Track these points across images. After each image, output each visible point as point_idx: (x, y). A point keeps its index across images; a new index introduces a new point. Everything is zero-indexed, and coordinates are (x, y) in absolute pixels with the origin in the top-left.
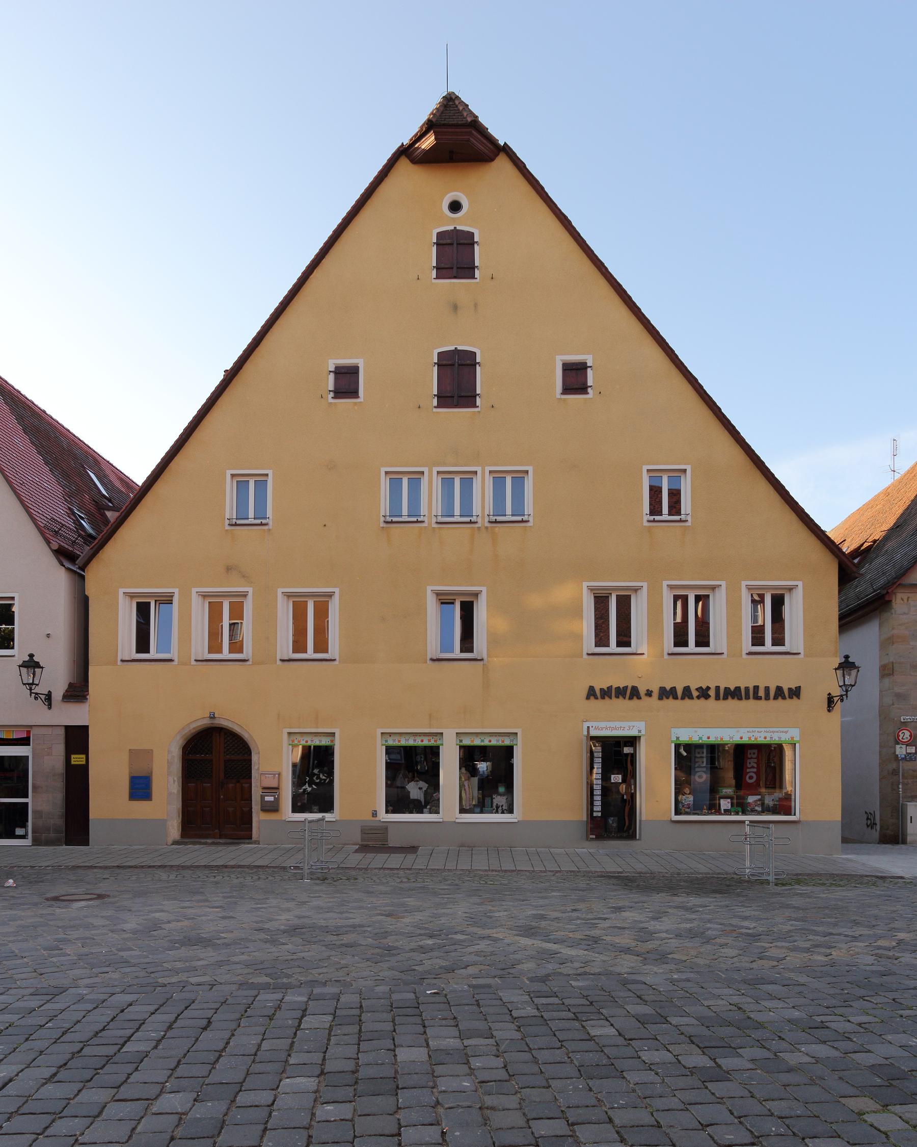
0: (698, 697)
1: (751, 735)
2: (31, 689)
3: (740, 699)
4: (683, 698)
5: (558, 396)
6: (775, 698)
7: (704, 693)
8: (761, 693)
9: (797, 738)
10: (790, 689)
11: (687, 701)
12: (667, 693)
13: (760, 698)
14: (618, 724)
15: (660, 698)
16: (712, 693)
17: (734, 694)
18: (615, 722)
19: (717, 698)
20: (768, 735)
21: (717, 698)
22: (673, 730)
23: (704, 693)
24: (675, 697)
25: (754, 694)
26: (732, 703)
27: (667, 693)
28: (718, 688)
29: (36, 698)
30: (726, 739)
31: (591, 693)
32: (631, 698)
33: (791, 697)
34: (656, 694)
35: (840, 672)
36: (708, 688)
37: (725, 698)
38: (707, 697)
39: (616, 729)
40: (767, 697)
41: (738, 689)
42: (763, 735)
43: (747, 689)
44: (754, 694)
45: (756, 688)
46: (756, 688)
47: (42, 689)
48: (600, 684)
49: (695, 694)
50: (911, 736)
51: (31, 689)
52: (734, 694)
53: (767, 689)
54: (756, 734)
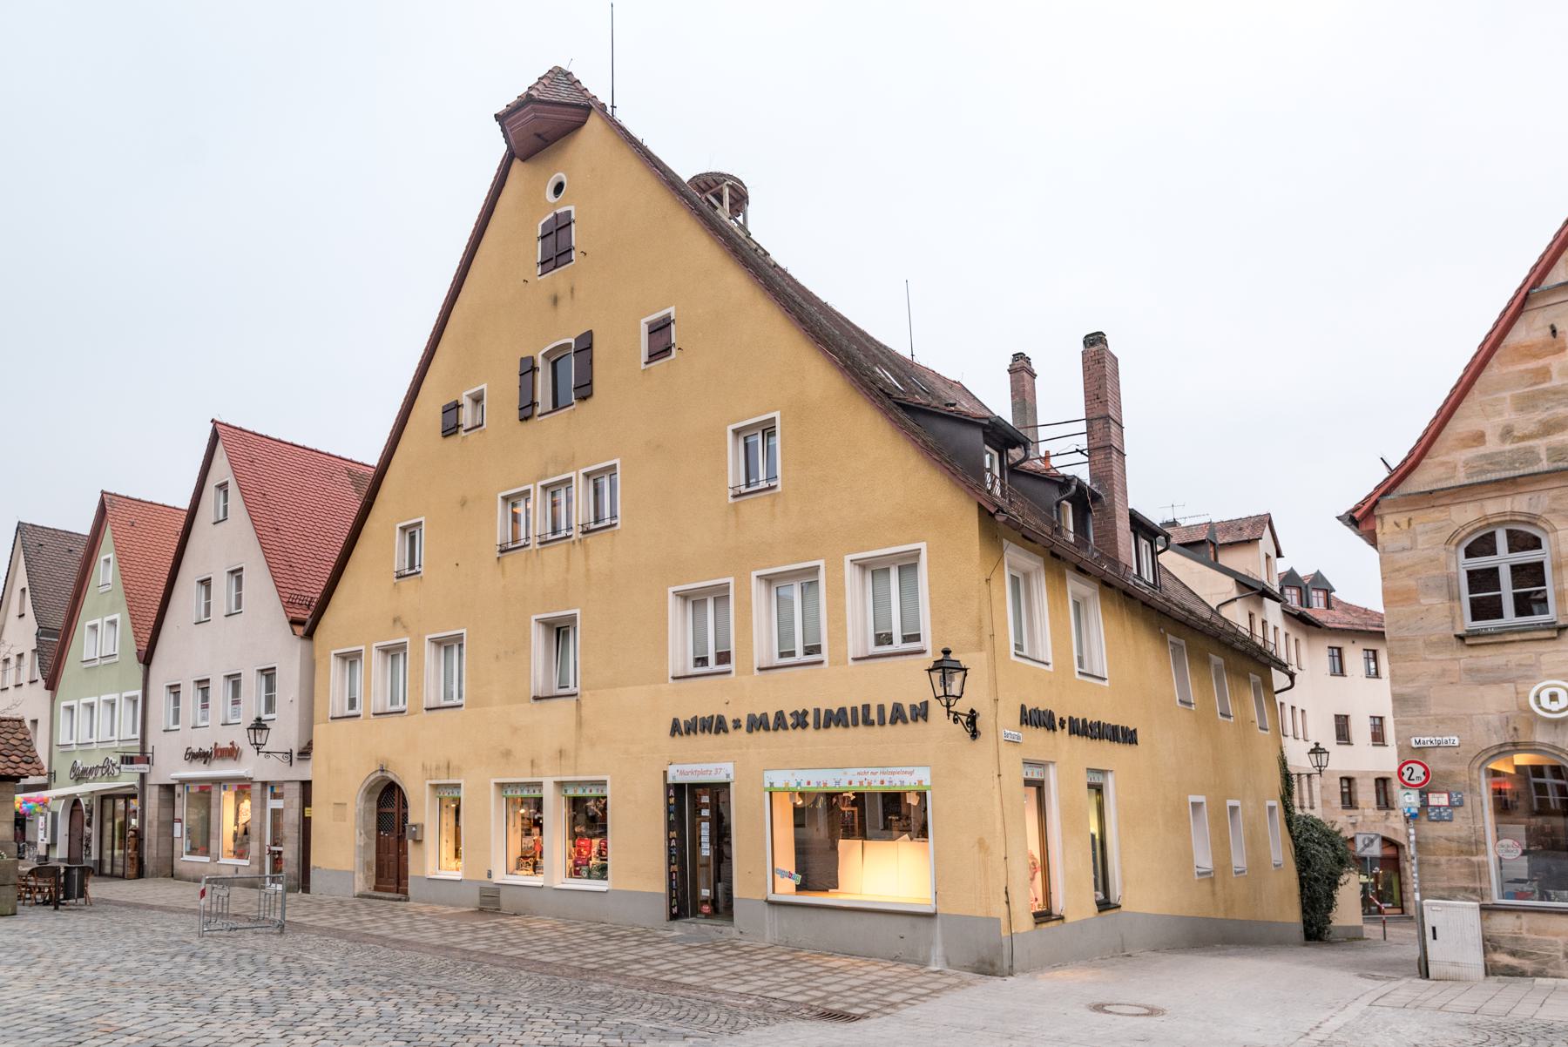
0: (794, 727)
1: (862, 778)
2: (948, 706)
3: (846, 726)
4: (776, 729)
5: (643, 366)
6: (893, 721)
7: (800, 720)
8: (874, 716)
9: (927, 783)
10: (913, 707)
11: (781, 731)
12: (757, 723)
13: (872, 723)
14: (705, 767)
15: (750, 730)
16: (810, 719)
17: (836, 719)
18: (702, 763)
19: (817, 726)
20: (886, 778)
21: (817, 726)
22: (767, 774)
23: (800, 720)
24: (767, 728)
25: (862, 717)
26: (836, 732)
27: (757, 723)
28: (817, 711)
29: (955, 721)
30: (844, 785)
31: (675, 728)
32: (717, 732)
33: (915, 720)
34: (744, 723)
35: (937, 676)
36: (805, 713)
37: (827, 726)
38: (804, 725)
39: (702, 773)
40: (882, 723)
41: (843, 710)
42: (879, 777)
43: (854, 710)
44: (862, 717)
45: (866, 708)
46: (866, 708)
47: (961, 707)
48: (684, 716)
49: (790, 721)
50: (1426, 773)
51: (948, 706)
52: (836, 719)
53: (881, 708)
54: (869, 777)
